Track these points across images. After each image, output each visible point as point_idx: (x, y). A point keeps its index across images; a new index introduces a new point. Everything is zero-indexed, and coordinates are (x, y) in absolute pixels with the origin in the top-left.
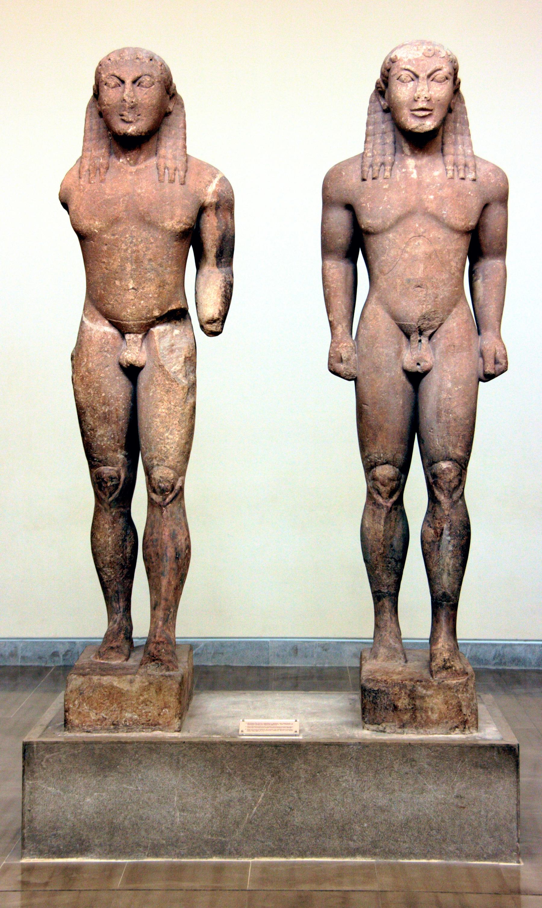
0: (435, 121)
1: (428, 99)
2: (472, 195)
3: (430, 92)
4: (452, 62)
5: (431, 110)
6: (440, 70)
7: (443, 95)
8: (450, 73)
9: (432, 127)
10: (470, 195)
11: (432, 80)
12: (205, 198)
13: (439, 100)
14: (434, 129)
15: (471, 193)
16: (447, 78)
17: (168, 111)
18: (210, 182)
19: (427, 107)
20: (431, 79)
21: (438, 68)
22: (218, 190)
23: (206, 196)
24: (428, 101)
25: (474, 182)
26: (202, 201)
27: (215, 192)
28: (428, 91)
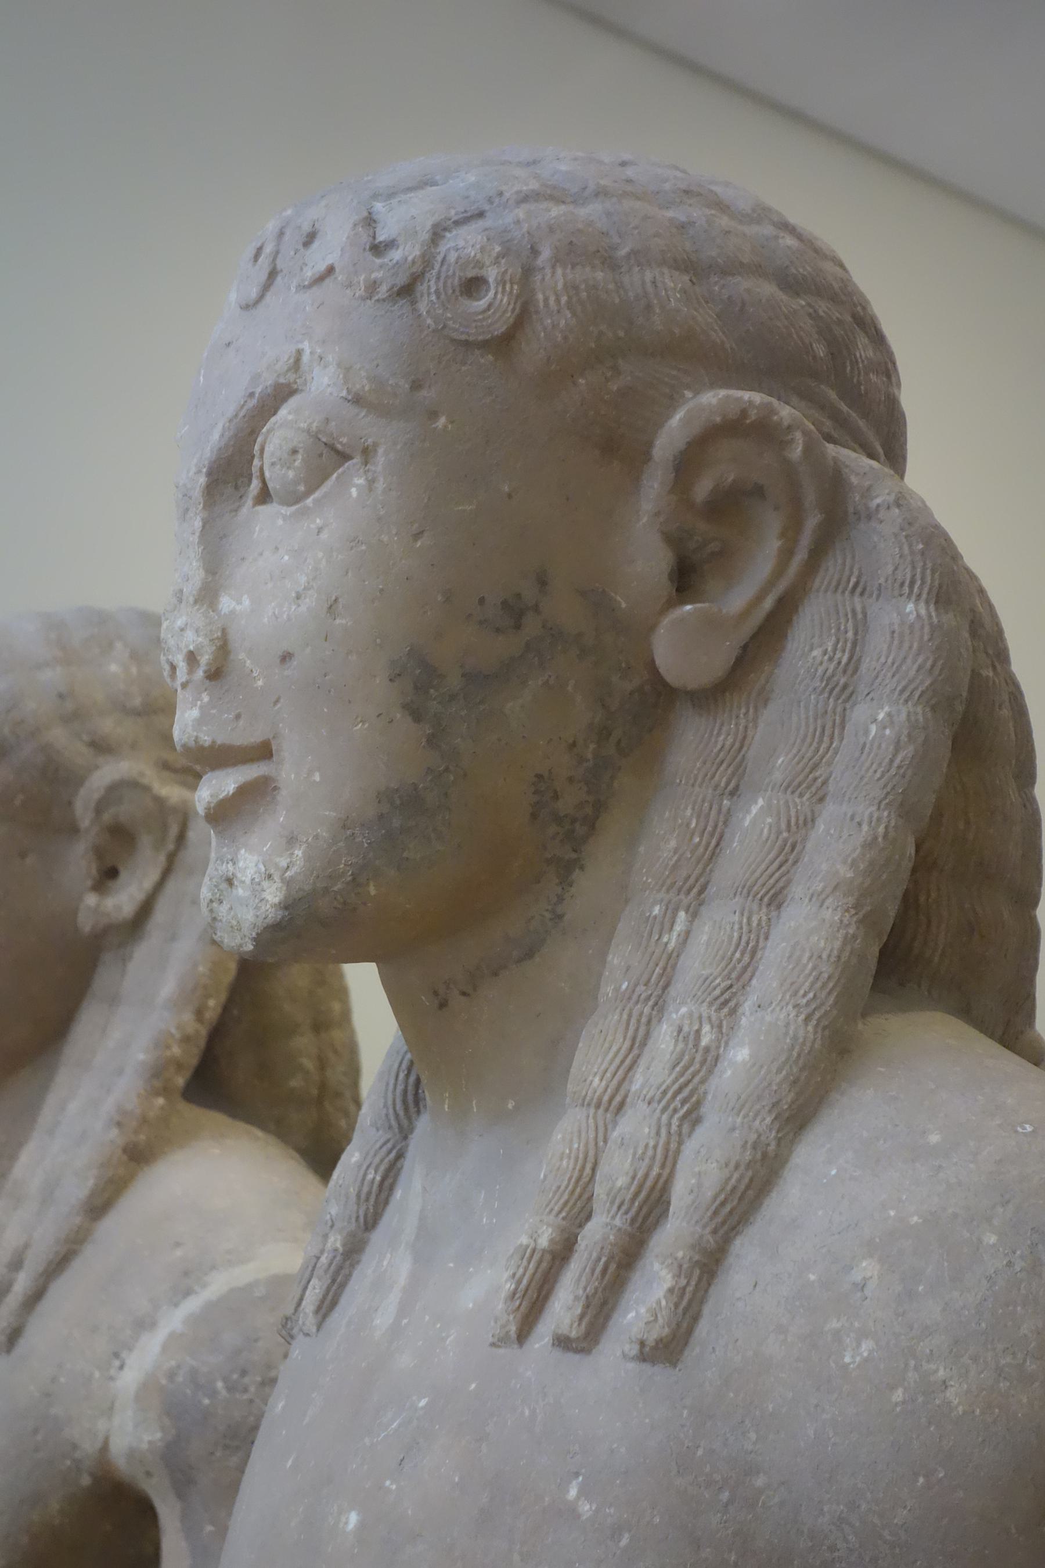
0: (291, 841)
1: (204, 659)
2: (586, 1508)
3: (226, 603)
4: (406, 291)
5: (264, 752)
6: (280, 394)
7: (309, 601)
8: (357, 400)
9: (273, 895)
10: (571, 1512)
11: (265, 496)
12: (101, 1425)
13: (286, 658)
14: (286, 906)
15: (583, 1492)
16: (329, 456)
17: (86, 923)
18: (144, 1324)
19: (206, 740)
20: (255, 485)
21: (268, 380)
22: (171, 1375)
23: (109, 1411)
24: (215, 674)
25: (659, 1373)
26: (89, 1447)
27: (147, 1387)
28: (208, 595)
